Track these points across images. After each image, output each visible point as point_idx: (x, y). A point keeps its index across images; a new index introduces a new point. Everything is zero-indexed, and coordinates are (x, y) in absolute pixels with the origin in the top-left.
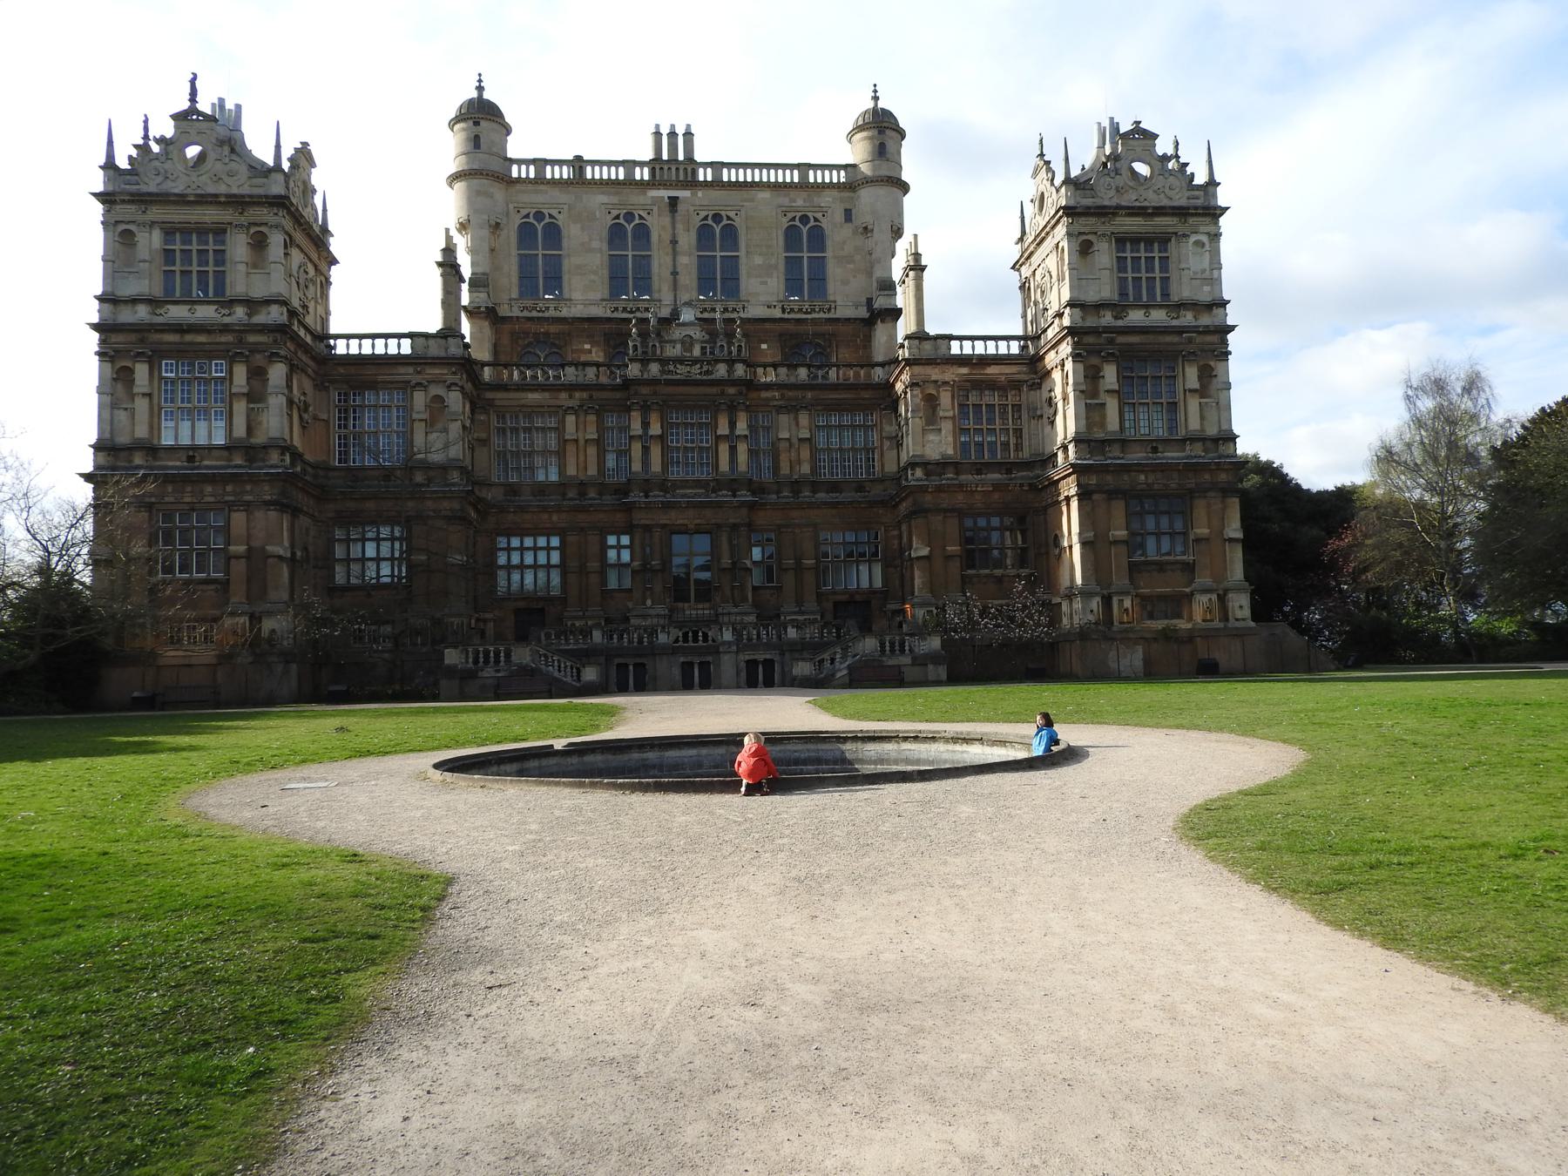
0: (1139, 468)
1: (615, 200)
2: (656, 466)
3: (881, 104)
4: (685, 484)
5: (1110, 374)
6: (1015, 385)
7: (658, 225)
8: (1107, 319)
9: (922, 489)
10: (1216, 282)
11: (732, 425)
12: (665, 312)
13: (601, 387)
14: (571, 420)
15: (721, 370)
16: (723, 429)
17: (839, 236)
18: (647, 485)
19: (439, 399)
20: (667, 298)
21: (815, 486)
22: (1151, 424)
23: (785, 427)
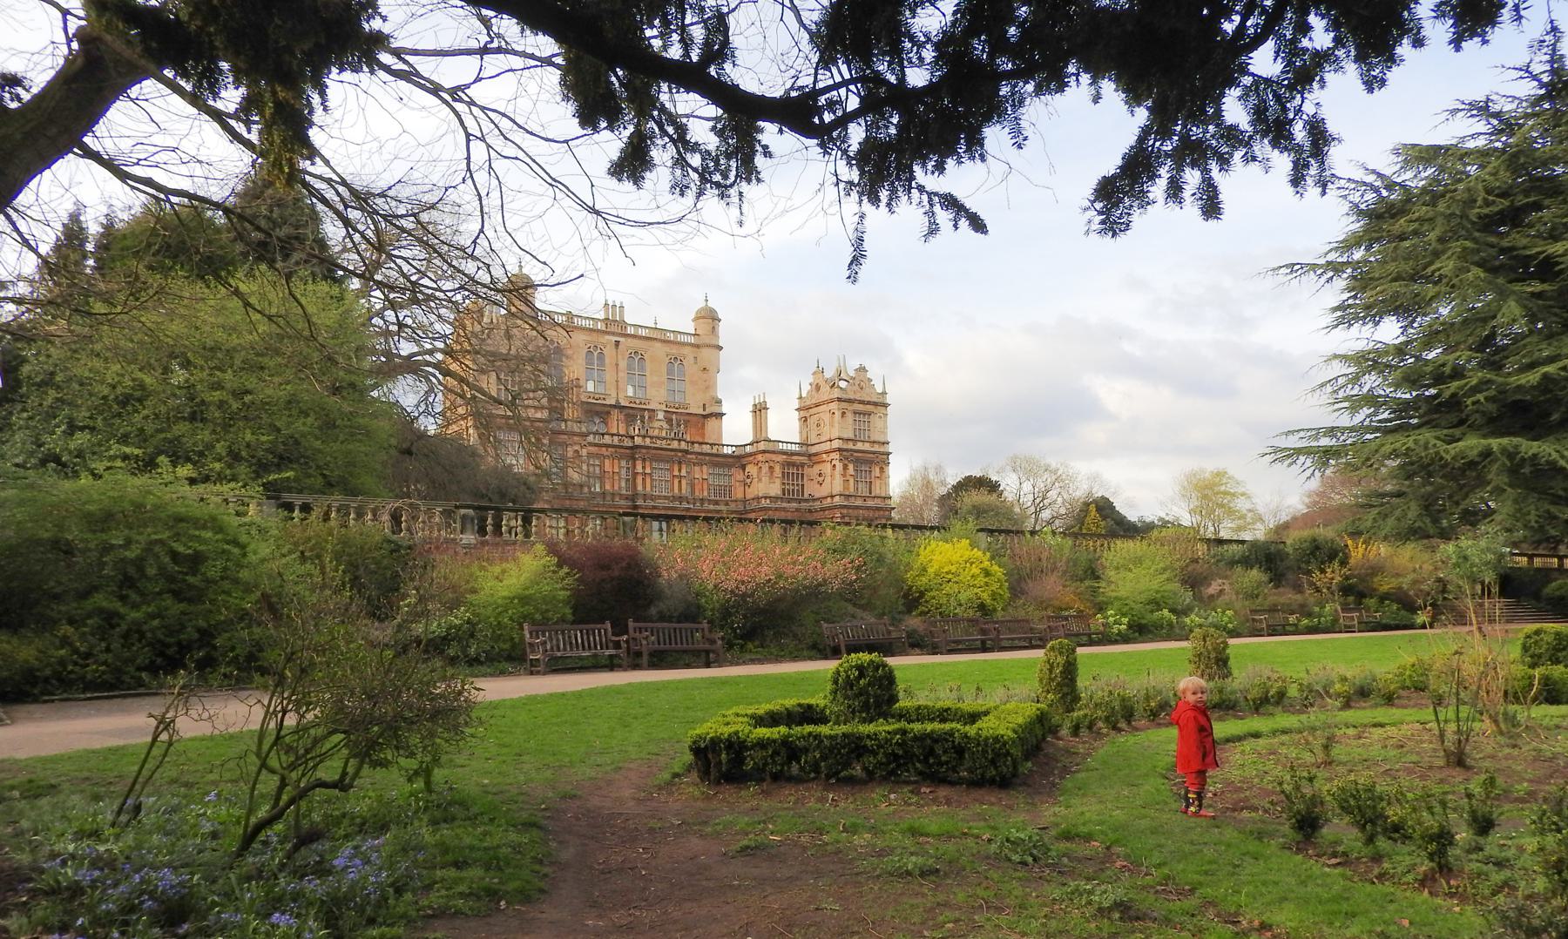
0: (857, 507)
1: (589, 338)
2: (648, 488)
3: (710, 304)
4: (660, 497)
5: (851, 467)
6: (802, 465)
7: (609, 352)
8: (850, 446)
9: (770, 509)
10: (885, 433)
11: (680, 471)
12: (613, 402)
13: (622, 447)
14: (607, 461)
15: (675, 445)
16: (676, 473)
17: (690, 367)
18: (645, 497)
19: (577, 451)
20: (614, 395)
21: (710, 501)
22: (863, 489)
23: (698, 473)
